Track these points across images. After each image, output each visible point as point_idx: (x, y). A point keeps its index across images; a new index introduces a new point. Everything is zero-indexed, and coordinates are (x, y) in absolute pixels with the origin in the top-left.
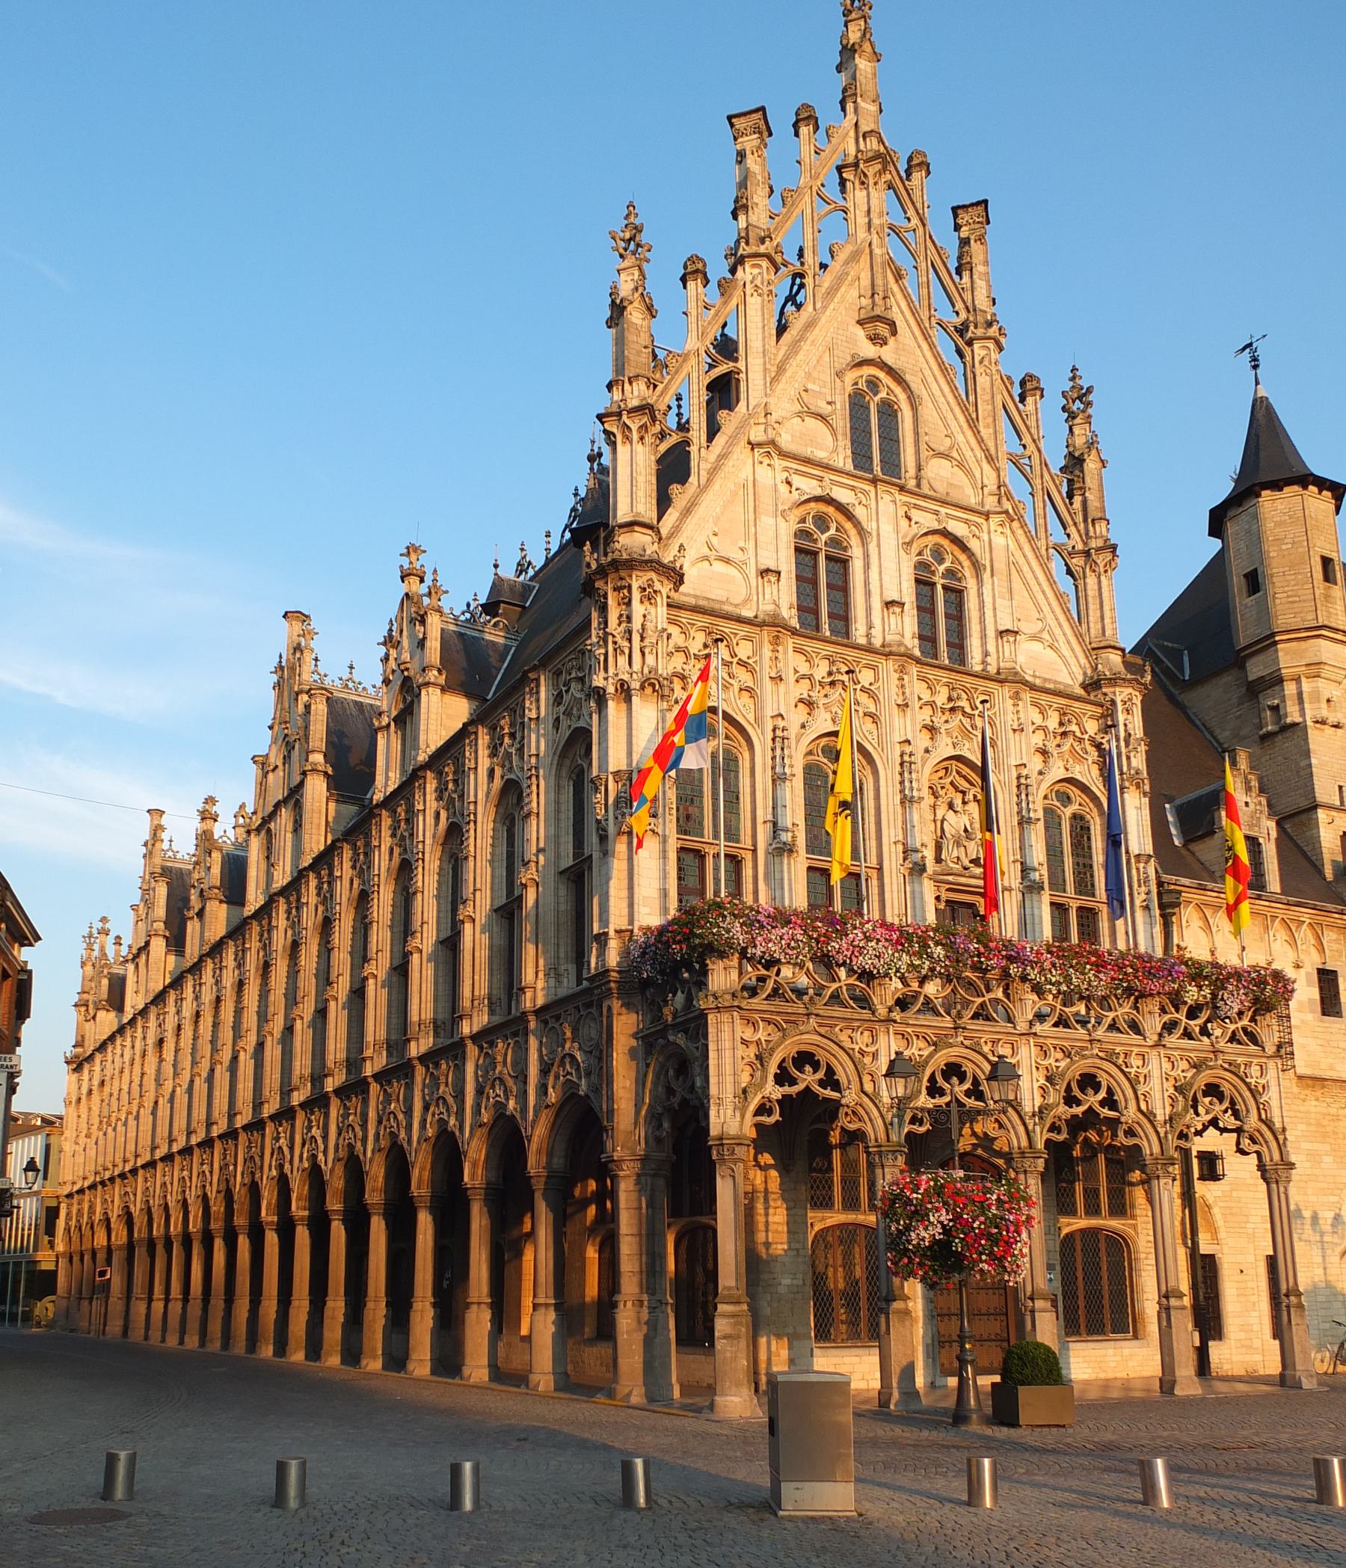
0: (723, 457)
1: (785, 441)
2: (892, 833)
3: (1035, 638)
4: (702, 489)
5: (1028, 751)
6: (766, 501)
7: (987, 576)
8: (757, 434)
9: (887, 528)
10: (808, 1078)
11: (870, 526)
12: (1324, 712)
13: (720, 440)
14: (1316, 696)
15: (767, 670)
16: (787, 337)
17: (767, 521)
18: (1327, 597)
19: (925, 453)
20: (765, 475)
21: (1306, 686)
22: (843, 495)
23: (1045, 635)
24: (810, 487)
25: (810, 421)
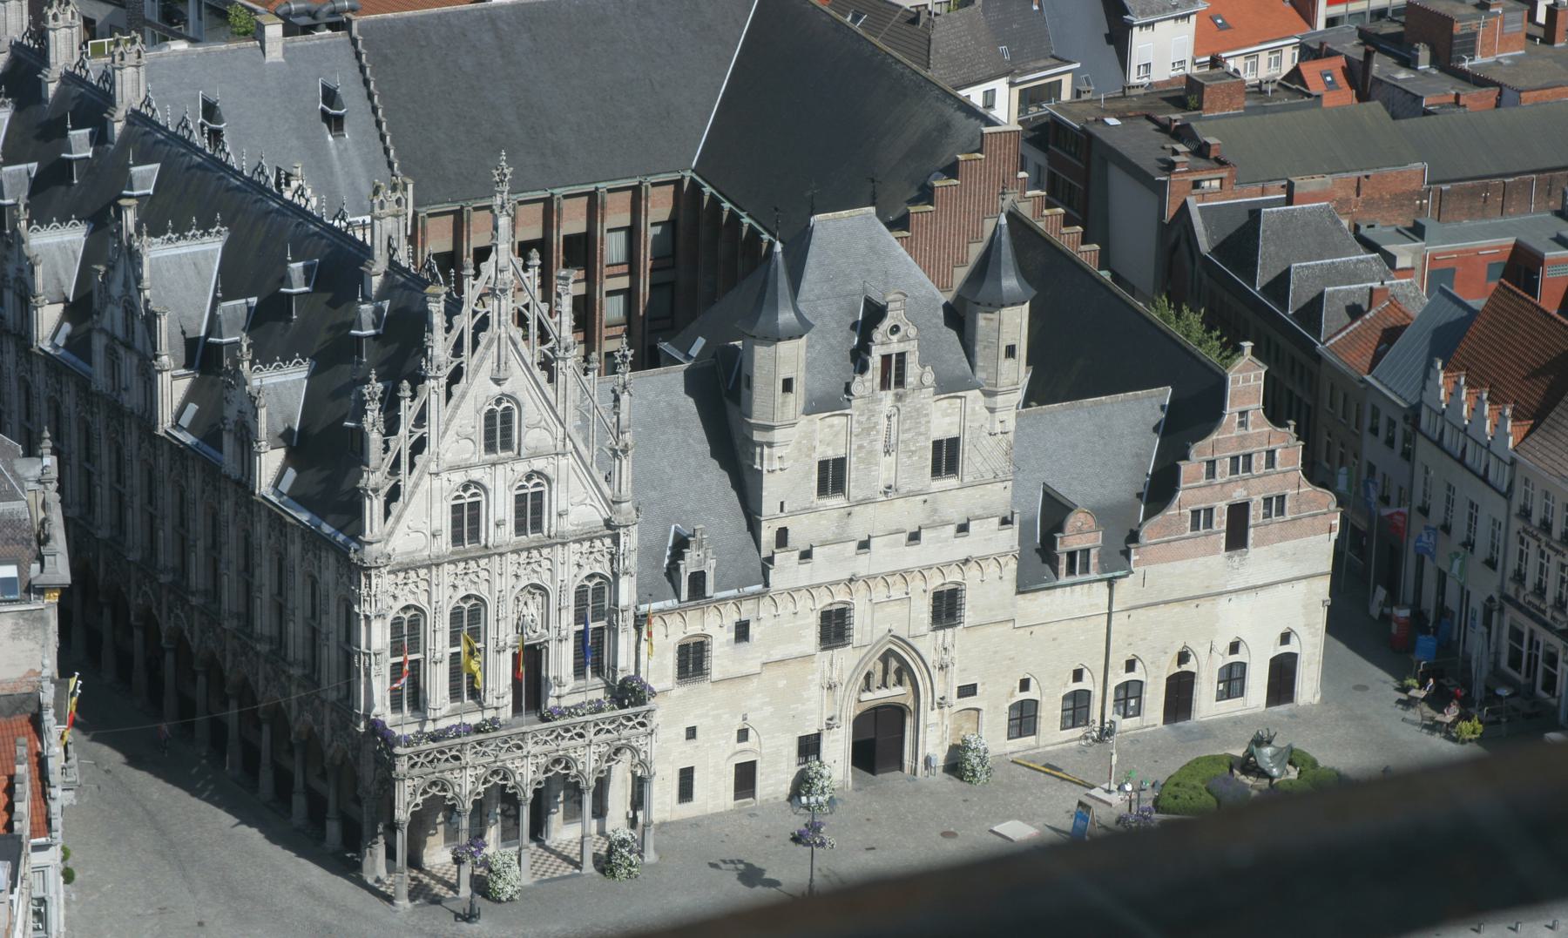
0: (416, 485)
1: (449, 458)
2: (491, 633)
3: (582, 503)
4: (406, 505)
5: (568, 570)
6: (437, 495)
7: (554, 485)
8: (433, 468)
9: (500, 483)
10: (434, 790)
11: (489, 486)
12: (777, 465)
13: (416, 472)
14: (771, 458)
15: (434, 581)
16: (452, 402)
17: (437, 506)
18: (784, 404)
19: (524, 429)
20: (436, 483)
21: (766, 450)
22: (476, 475)
23: (588, 501)
24: (459, 478)
25: (463, 442)
